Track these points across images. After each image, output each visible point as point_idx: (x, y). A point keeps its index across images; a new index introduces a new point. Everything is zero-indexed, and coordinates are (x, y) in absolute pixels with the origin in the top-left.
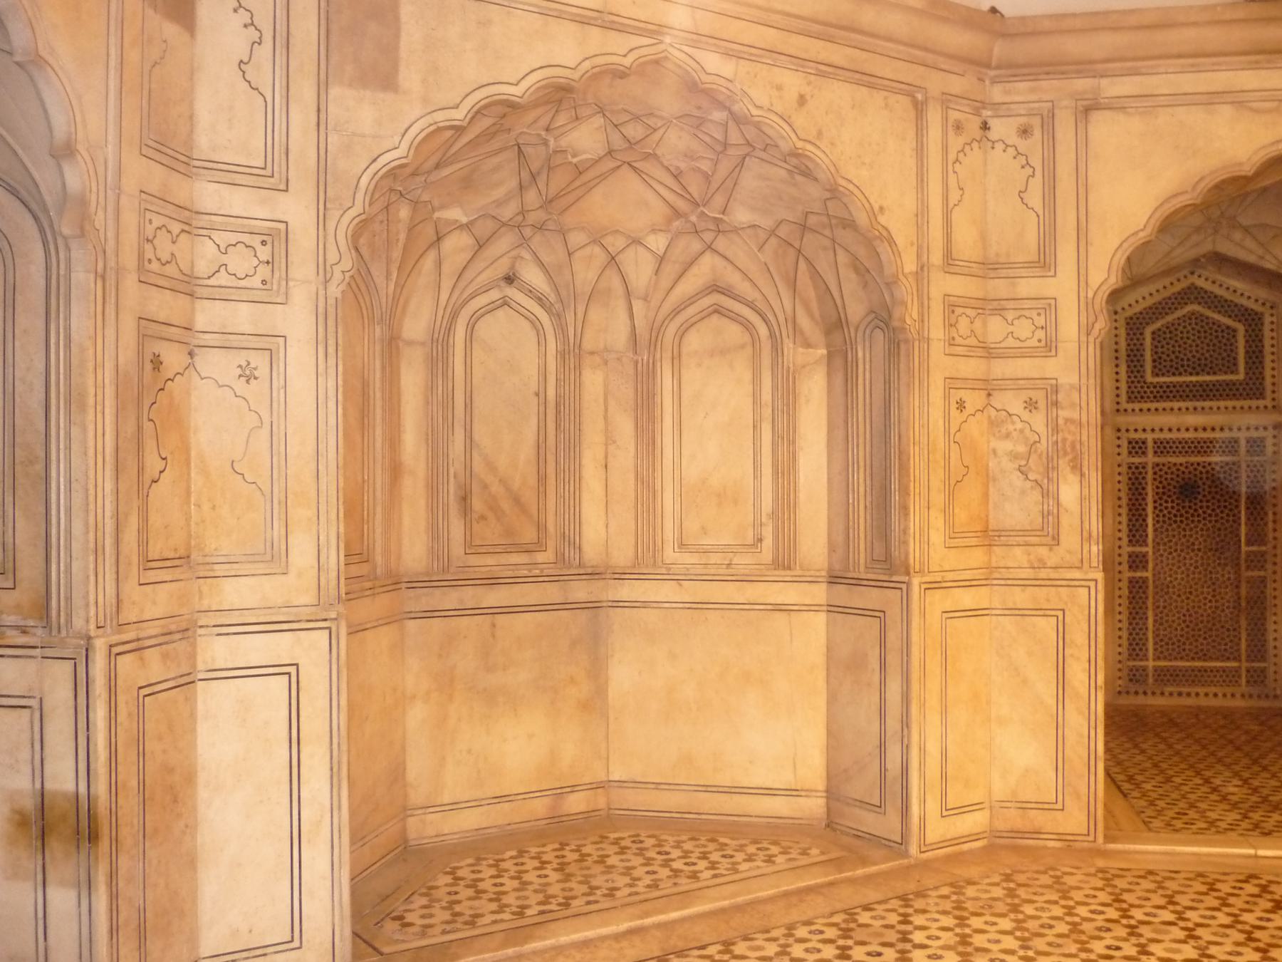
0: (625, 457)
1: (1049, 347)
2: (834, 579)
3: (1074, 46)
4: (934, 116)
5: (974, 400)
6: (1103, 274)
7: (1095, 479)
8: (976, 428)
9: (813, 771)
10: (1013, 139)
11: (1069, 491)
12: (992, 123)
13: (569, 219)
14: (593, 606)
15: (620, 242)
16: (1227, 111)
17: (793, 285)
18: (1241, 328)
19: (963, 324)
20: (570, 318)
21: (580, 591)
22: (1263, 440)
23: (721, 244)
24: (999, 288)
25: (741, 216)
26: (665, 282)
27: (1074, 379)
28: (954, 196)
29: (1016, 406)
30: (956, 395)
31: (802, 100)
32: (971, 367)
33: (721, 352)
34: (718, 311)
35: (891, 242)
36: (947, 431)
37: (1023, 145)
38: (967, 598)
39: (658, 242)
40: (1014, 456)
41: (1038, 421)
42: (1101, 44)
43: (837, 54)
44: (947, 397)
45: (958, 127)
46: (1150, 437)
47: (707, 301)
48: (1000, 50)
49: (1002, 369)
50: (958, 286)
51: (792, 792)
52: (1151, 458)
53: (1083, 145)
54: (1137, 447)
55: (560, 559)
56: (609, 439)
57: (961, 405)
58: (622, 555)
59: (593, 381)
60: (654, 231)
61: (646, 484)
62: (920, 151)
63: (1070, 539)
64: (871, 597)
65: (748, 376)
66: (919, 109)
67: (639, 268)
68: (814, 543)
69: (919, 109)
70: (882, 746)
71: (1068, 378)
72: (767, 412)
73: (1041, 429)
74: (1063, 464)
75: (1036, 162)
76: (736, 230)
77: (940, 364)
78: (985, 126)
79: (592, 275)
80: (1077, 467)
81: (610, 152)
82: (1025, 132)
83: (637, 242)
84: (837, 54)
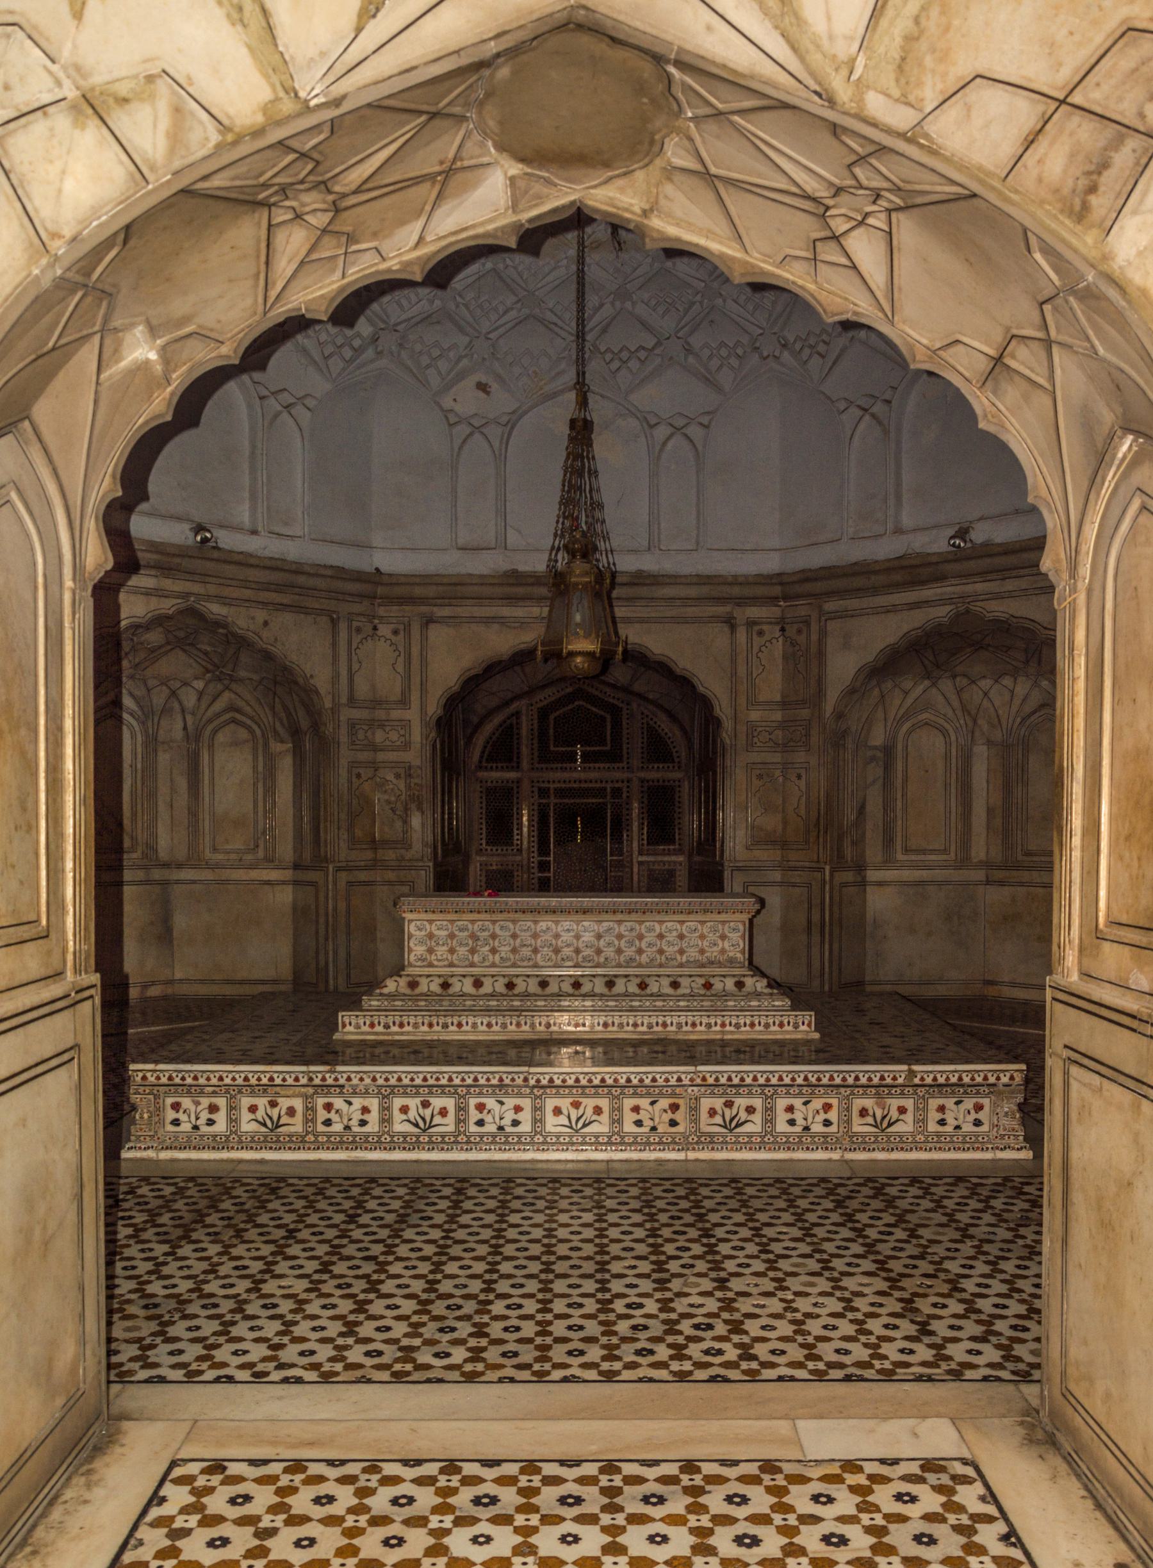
0: (182, 799)
1: (406, 746)
2: (296, 866)
3: (418, 591)
4: (343, 626)
5: (366, 773)
6: (434, 708)
7: (429, 813)
8: (367, 787)
9: (285, 969)
10: (389, 635)
11: (416, 821)
12: (380, 626)
13: (149, 672)
14: (165, 883)
15: (178, 684)
16: (496, 626)
17: (273, 708)
18: (608, 717)
19: (361, 735)
20: (150, 724)
21: (157, 874)
22: (619, 789)
23: (234, 686)
24: (380, 714)
25: (243, 674)
26: (203, 706)
27: (418, 762)
28: (355, 666)
29: (390, 777)
30: (355, 771)
31: (266, 623)
32: (364, 756)
33: (236, 744)
34: (234, 721)
35: (317, 692)
36: (350, 789)
37: (393, 638)
38: (363, 876)
39: (199, 684)
40: (388, 802)
41: (402, 785)
42: (431, 591)
43: (285, 599)
44: (349, 772)
45: (358, 630)
46: (552, 786)
47: (227, 716)
48: (380, 590)
49: (381, 756)
50: (356, 714)
51: (275, 982)
52: (553, 800)
53: (424, 638)
54: (543, 792)
55: (145, 856)
56: (173, 790)
57: (359, 776)
58: (181, 854)
59: (164, 758)
60: (196, 678)
61: (193, 814)
62: (334, 645)
63: (417, 846)
64: (311, 876)
65: (250, 758)
66: (334, 623)
67: (189, 699)
68: (286, 850)
69: (334, 623)
70: (317, 953)
71: (418, 762)
72: (261, 776)
73: (402, 786)
74: (413, 806)
75: (401, 649)
76: (241, 680)
77: (345, 756)
78: (375, 628)
79: (162, 701)
80: (420, 808)
81: (168, 643)
82: (396, 632)
83: (186, 684)
84: (285, 599)
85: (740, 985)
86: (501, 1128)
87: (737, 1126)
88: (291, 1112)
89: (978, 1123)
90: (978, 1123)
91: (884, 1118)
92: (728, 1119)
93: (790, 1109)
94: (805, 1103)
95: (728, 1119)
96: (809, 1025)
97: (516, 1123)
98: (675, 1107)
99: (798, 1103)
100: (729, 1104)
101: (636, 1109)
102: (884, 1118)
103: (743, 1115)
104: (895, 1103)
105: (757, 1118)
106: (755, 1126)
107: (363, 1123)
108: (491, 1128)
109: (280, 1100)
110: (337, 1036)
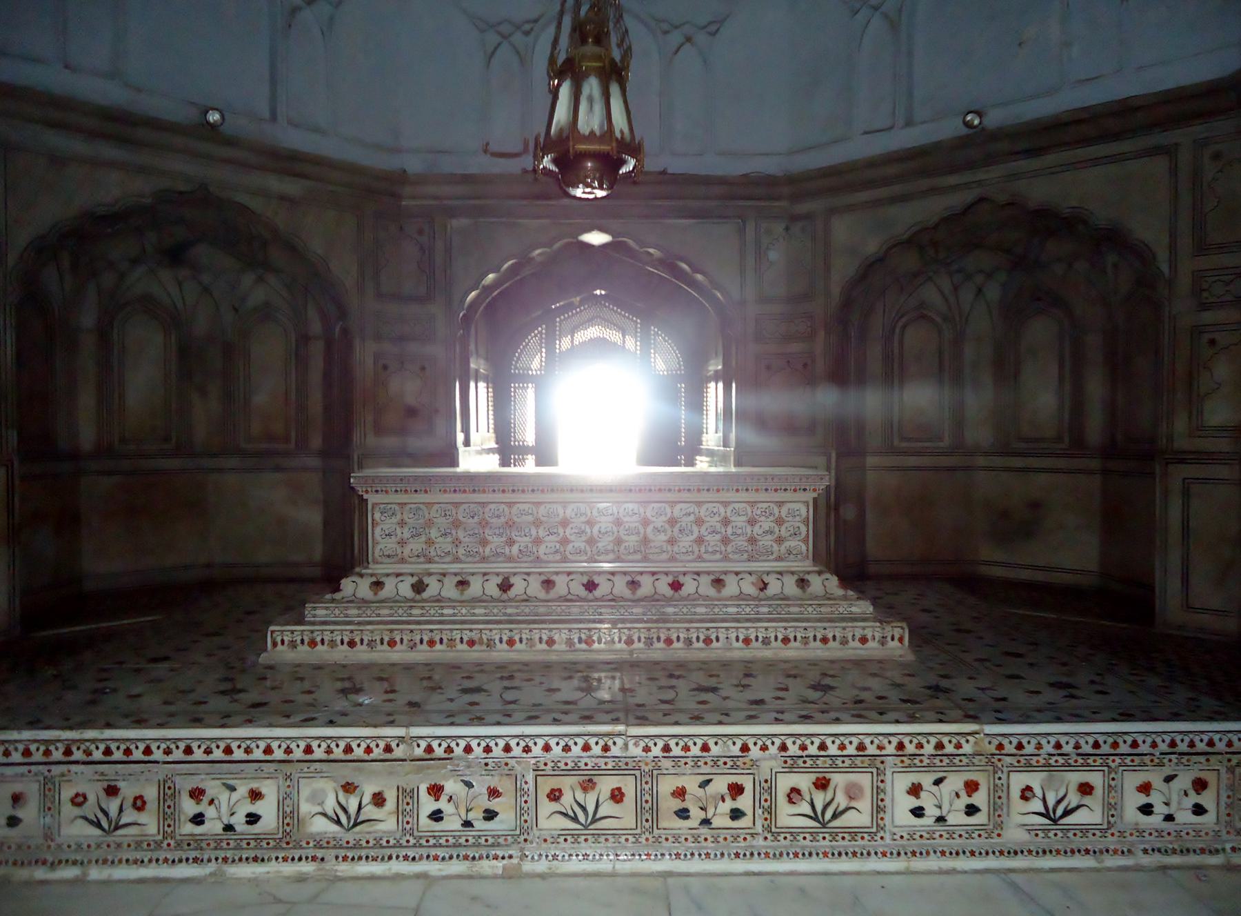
85: (802, 583)
86: (467, 824)
87: (835, 816)
88: (139, 804)
89: (1199, 810)
90: (1199, 810)
91: (1059, 802)
92: (819, 808)
93: (915, 790)
94: (938, 782)
95: (819, 808)
96: (901, 640)
97: (490, 815)
98: (736, 790)
99: (927, 780)
100: (822, 784)
101: (680, 793)
102: (1059, 802)
103: (841, 801)
104: (1075, 778)
105: (865, 804)
106: (860, 817)
107: (253, 819)
108: (452, 823)
109: (121, 784)
110: (264, 658)
